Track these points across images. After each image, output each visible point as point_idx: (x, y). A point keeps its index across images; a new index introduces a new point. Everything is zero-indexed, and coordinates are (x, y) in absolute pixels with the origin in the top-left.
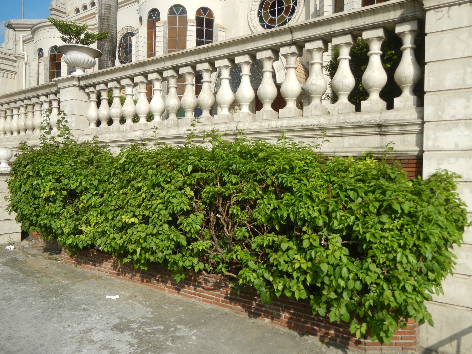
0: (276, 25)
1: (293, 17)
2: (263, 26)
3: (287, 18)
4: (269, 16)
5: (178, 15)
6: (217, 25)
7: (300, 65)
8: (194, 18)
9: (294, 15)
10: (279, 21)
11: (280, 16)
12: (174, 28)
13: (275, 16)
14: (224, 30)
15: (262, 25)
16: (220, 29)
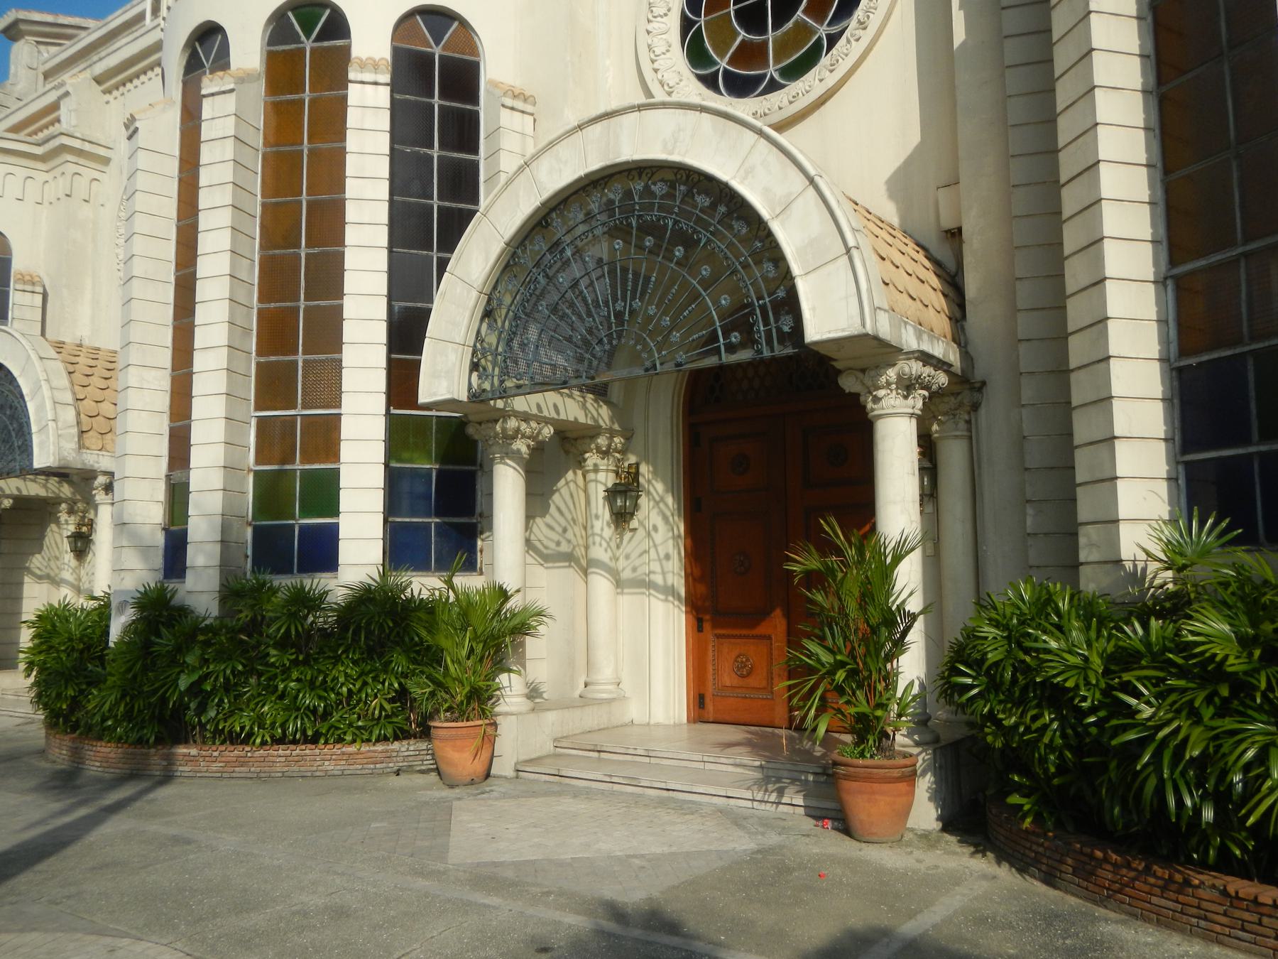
0: (772, 70)
1: (853, 22)
2: (710, 82)
3: (823, 30)
4: (737, 34)
5: (308, 45)
6: (494, 84)
7: (911, 249)
8: (383, 51)
9: (859, 13)
10: (782, 50)
11: (790, 24)
12: (293, 102)
13: (764, 31)
14: (529, 108)
15: (701, 78)
16: (509, 102)
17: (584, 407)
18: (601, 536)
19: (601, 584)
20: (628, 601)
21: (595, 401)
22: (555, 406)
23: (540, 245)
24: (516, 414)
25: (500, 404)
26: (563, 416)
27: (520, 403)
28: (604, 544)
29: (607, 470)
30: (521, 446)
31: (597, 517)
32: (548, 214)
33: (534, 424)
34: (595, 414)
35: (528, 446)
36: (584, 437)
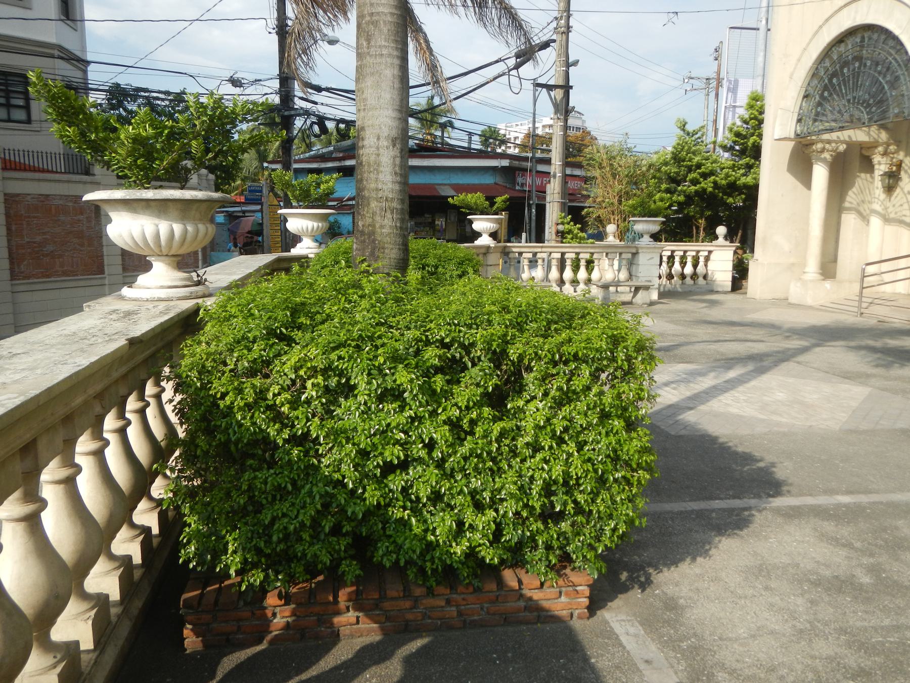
17: (869, 134)
18: (879, 200)
19: (875, 221)
20: (890, 229)
21: (878, 130)
22: (849, 137)
23: (827, 63)
24: (822, 141)
25: (814, 138)
26: (854, 139)
27: (826, 136)
28: (880, 203)
29: (886, 164)
30: (827, 155)
31: (877, 188)
32: (830, 49)
33: (833, 145)
34: (876, 136)
35: (831, 155)
36: (872, 147)
